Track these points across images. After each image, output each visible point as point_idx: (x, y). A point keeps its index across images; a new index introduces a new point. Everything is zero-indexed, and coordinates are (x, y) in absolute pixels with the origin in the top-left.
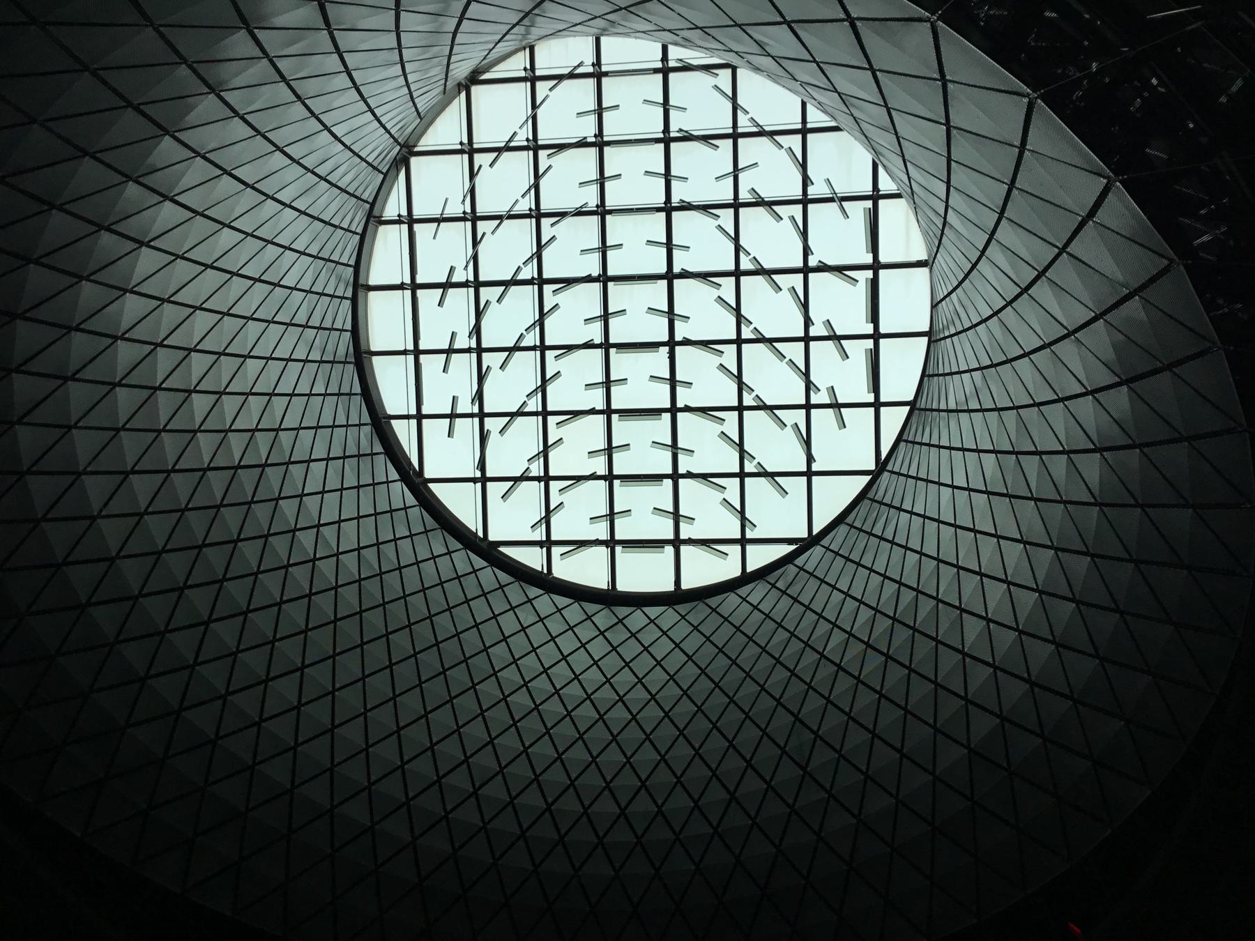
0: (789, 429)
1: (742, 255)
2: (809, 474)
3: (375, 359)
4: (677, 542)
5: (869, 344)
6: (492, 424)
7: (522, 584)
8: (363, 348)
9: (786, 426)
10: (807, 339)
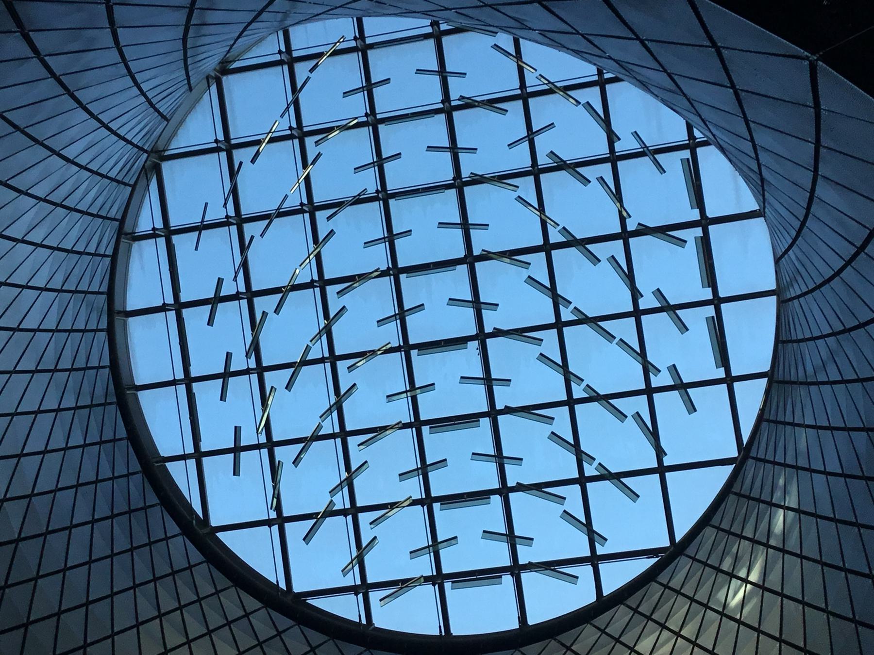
0: (630, 420)
1: (550, 228)
2: (661, 470)
3: (143, 396)
4: (516, 569)
5: (710, 311)
6: (284, 454)
7: (339, 642)
8: (125, 381)
9: (626, 417)
10: (637, 313)
